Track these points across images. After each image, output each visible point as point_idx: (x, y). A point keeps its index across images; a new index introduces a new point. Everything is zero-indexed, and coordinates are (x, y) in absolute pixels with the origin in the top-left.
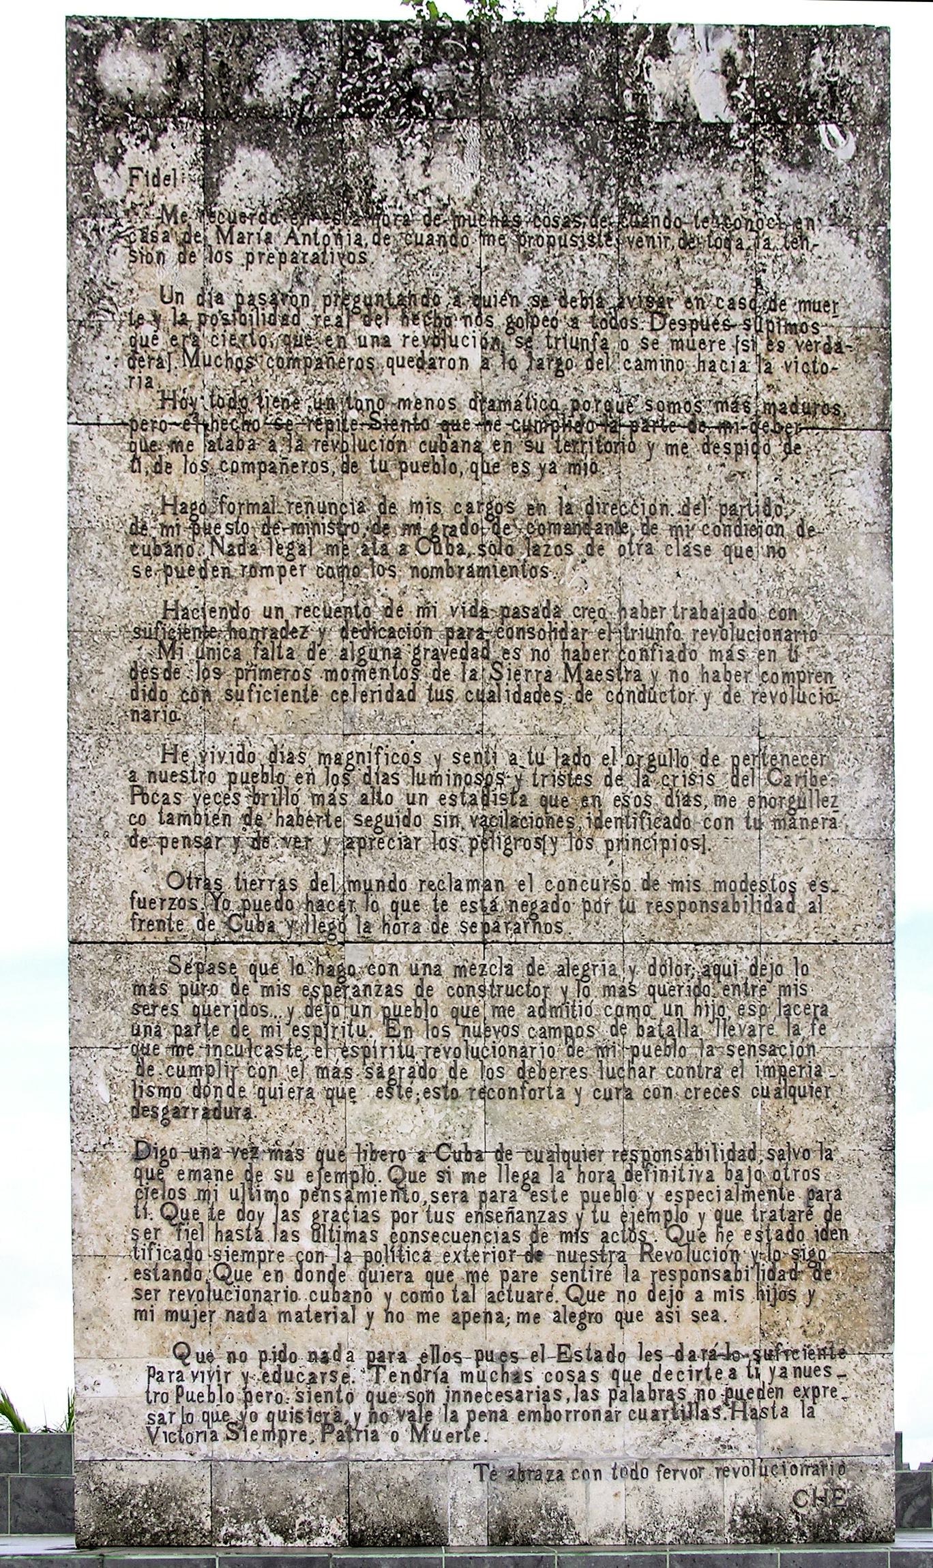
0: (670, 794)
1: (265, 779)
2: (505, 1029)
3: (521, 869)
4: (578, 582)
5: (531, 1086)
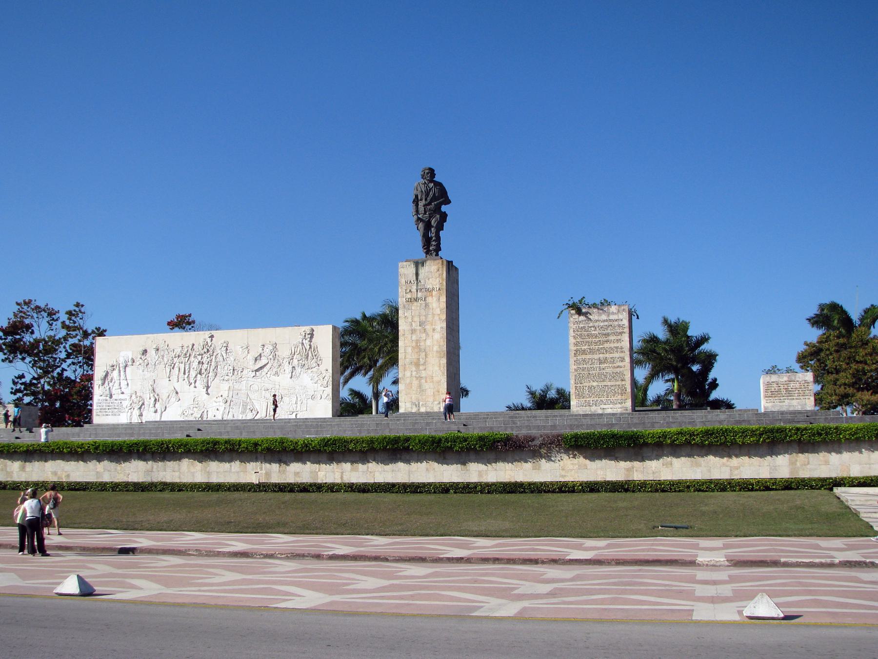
0: (613, 360)
1: (584, 360)
2: (602, 377)
3: (602, 366)
4: (606, 345)
5: (604, 381)
